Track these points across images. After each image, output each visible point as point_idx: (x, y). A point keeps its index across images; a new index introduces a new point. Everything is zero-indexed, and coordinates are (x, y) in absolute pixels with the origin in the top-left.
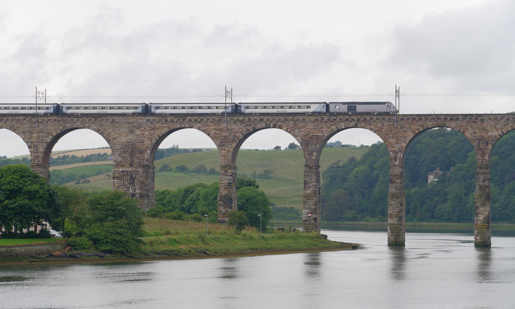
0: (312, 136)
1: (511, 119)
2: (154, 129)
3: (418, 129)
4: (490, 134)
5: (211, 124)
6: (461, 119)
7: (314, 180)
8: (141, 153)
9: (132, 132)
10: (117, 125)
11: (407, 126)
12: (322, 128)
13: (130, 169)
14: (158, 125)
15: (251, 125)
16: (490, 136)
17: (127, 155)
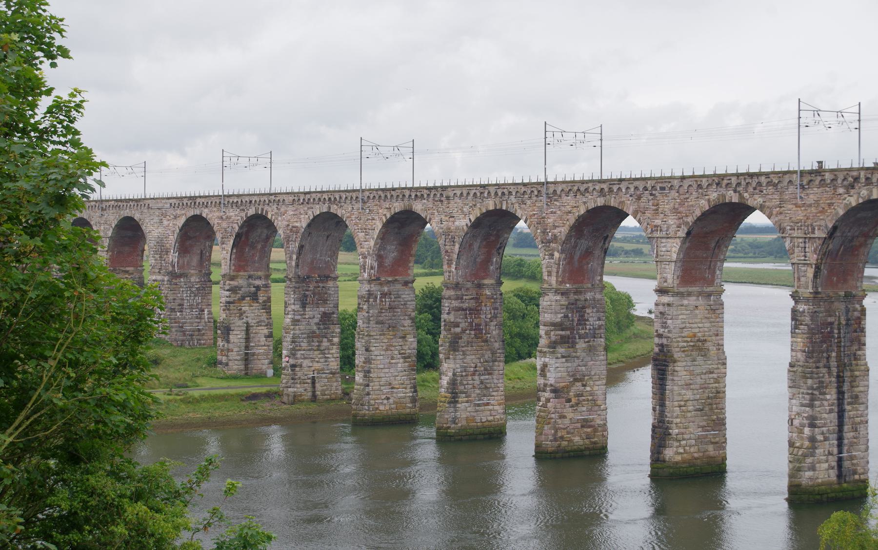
0: (293, 227)
1: (478, 194)
2: (176, 217)
3: (385, 215)
4: (457, 223)
5: (215, 209)
6: (425, 196)
7: (292, 301)
8: (167, 252)
9: (161, 222)
10: (152, 211)
11: (375, 208)
12: (301, 214)
13: (159, 278)
14: (178, 212)
15: (244, 210)
16: (457, 228)
17: (157, 256)
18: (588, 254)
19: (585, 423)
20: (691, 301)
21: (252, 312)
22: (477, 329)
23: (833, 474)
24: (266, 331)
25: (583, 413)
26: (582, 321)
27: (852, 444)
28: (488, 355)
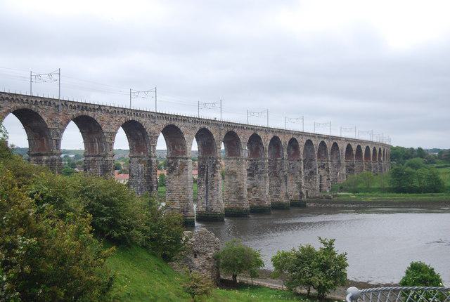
18: (257, 149)
19: (258, 200)
20: (232, 161)
21: (323, 172)
22: (275, 173)
23: (204, 209)
24: (327, 178)
25: (257, 196)
26: (257, 169)
27: (211, 201)
28: (278, 181)
